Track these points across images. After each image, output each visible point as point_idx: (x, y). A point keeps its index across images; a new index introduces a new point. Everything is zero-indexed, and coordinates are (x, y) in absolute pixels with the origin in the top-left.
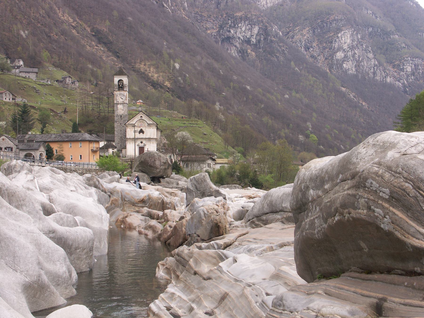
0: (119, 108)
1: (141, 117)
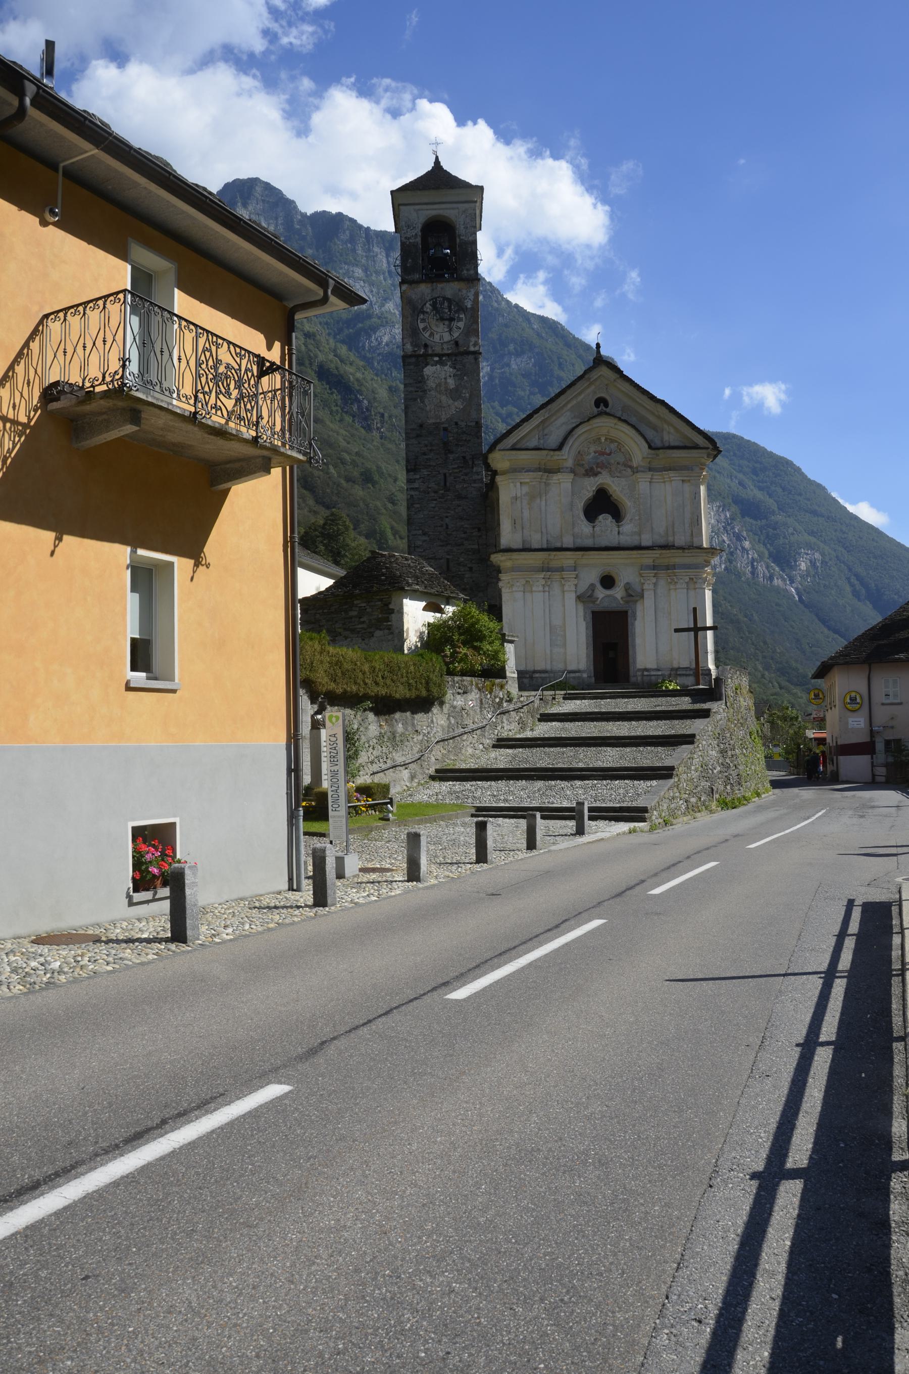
0: (431, 384)
1: (601, 402)
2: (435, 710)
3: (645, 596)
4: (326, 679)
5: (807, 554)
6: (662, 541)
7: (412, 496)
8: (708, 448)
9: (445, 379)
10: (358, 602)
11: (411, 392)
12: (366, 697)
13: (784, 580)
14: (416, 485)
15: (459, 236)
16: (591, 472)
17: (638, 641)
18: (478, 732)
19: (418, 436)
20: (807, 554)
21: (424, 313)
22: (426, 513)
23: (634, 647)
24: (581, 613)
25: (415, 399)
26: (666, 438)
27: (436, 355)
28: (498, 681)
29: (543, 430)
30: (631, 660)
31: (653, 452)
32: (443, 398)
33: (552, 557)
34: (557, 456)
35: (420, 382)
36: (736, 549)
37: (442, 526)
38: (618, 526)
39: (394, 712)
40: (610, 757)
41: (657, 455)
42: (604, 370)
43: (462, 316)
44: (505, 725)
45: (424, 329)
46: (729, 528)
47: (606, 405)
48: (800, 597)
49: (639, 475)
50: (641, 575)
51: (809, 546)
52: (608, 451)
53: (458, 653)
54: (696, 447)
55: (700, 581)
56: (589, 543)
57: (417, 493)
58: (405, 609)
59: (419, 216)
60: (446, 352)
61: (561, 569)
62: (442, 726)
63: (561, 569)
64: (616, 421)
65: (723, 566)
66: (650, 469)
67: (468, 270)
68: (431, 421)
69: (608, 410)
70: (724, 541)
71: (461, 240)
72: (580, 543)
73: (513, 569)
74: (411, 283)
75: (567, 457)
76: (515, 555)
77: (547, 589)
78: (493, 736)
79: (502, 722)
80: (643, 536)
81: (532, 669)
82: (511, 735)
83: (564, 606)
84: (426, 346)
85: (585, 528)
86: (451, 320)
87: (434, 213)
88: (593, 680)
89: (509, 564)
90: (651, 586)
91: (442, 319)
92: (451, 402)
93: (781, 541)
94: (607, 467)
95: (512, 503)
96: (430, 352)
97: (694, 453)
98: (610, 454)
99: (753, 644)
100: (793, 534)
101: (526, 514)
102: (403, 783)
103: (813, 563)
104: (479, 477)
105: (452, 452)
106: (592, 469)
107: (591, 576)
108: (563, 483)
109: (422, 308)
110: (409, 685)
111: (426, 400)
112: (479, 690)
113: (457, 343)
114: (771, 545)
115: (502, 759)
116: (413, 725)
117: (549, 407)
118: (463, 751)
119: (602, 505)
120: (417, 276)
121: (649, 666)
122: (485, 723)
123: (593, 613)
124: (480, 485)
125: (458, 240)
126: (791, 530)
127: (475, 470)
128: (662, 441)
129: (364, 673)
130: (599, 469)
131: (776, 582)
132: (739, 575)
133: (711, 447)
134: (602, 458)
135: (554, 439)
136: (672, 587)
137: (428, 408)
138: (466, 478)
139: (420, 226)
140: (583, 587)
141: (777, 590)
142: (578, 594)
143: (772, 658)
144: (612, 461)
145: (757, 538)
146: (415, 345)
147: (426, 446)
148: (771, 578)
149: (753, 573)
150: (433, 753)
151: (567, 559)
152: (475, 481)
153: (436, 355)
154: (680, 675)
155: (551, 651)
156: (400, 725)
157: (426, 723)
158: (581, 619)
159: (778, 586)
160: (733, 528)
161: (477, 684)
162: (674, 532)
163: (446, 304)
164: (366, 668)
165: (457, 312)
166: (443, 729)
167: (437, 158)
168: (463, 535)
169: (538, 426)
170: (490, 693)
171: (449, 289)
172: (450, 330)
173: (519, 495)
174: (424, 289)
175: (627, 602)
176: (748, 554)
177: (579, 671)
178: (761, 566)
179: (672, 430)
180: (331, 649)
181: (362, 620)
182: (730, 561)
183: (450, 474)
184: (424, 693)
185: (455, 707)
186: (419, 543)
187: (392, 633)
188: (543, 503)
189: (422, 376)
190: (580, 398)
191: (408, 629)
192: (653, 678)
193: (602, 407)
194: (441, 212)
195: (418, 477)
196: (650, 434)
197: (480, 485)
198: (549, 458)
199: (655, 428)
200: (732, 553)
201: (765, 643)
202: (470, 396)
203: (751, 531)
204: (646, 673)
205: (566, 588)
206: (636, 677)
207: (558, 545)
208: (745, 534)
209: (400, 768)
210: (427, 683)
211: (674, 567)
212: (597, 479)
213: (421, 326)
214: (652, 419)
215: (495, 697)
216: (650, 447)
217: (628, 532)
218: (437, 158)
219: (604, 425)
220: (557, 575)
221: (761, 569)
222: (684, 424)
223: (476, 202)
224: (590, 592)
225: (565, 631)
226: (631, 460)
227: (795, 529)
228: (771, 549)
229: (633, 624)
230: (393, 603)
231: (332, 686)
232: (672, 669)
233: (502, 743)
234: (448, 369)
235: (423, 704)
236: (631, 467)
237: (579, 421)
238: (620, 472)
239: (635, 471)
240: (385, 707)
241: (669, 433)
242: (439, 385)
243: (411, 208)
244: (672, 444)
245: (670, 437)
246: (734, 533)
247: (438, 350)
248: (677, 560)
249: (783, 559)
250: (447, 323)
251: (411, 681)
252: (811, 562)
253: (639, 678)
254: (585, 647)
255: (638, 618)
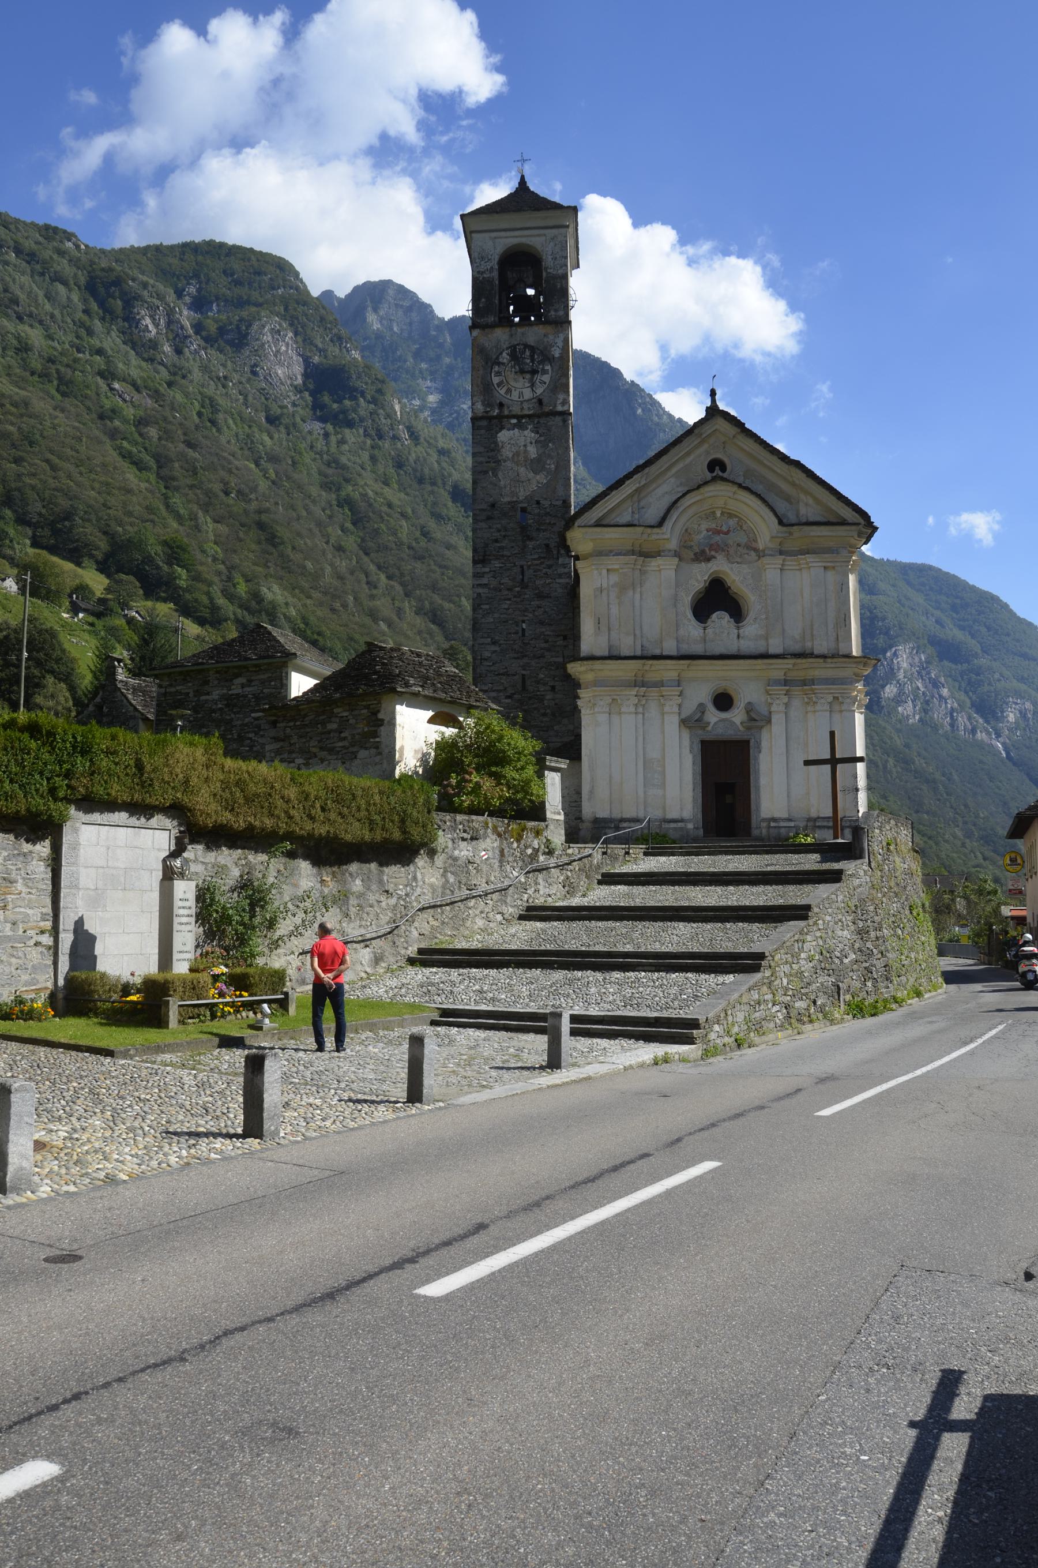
0: (507, 452)
1: (716, 465)
2: (421, 861)
3: (773, 720)
4: (213, 806)
5: (1016, 704)
6: (797, 648)
7: (479, 594)
8: (859, 524)
9: (525, 446)
10: (339, 710)
11: (481, 463)
12: (289, 836)
13: (988, 733)
14: (485, 581)
15: (546, 268)
16: (703, 556)
17: (763, 781)
18: (495, 896)
19: (489, 518)
20: (1016, 704)
21: (499, 364)
22: (496, 615)
23: (758, 788)
24: (686, 742)
25: (486, 472)
26: (803, 510)
27: (514, 417)
28: (531, 824)
29: (639, 501)
30: (753, 807)
31: (785, 529)
32: (522, 470)
33: (647, 668)
34: (656, 534)
35: (492, 450)
36: (933, 697)
37: (516, 633)
38: (738, 628)
39: (348, 861)
40: (678, 937)
41: (791, 534)
42: (720, 423)
43: (548, 367)
44: (541, 887)
45: (499, 385)
46: (924, 673)
47: (723, 468)
48: (1008, 754)
49: (766, 560)
50: (767, 692)
51: (1018, 694)
52: (725, 529)
53: (467, 781)
54: (843, 523)
55: (848, 700)
56: (698, 649)
57: (486, 590)
58: (399, 719)
59: (497, 246)
60: (526, 412)
61: (660, 684)
62: (432, 886)
63: (660, 684)
64: (735, 488)
65: (917, 717)
66: (781, 553)
67: (556, 311)
68: (506, 499)
69: (725, 475)
70: (918, 688)
71: (548, 273)
72: (686, 649)
73: (597, 683)
74: (483, 327)
75: (670, 536)
76: (598, 665)
77: (640, 710)
78: (520, 903)
79: (536, 884)
80: (771, 641)
81: (619, 816)
82: (550, 902)
83: (663, 732)
84: (501, 405)
85: (692, 629)
86: (534, 372)
87: (515, 241)
88: (701, 832)
89: (589, 677)
90: (782, 708)
91: (522, 372)
92: (531, 475)
93: (986, 688)
94: (723, 550)
95: (596, 597)
96: (506, 413)
97: (840, 531)
98: (727, 533)
99: (952, 807)
100: (999, 680)
101: (614, 610)
102: (359, 968)
103: (1023, 714)
104: (566, 570)
105: (531, 539)
106: (703, 552)
107: (701, 694)
108: (664, 570)
109: (497, 358)
110: (371, 822)
111: (500, 475)
112: (499, 835)
113: (540, 402)
114: (974, 692)
115: (521, 936)
116: (381, 882)
117: (647, 470)
118: (468, 923)
119: (716, 599)
120: (491, 319)
121: (777, 815)
122: (506, 883)
123: (703, 742)
124: (567, 580)
125: (544, 274)
126: (997, 676)
127: (560, 561)
128: (797, 516)
129: (288, 802)
130: (713, 553)
131: (980, 736)
132: (935, 728)
133: (862, 522)
134: (717, 538)
135: (653, 514)
136: (809, 708)
137: (502, 483)
138: (549, 571)
139: (497, 258)
140: (690, 708)
141: (981, 746)
142: (683, 716)
143: (975, 825)
144: (731, 542)
145: (957, 684)
146: (488, 404)
147: (499, 531)
148: (973, 731)
149: (952, 725)
150: (416, 924)
151: (668, 670)
152: (560, 576)
153: (514, 417)
154: (819, 827)
155: (645, 792)
156: (358, 882)
157: (404, 881)
158: (686, 751)
159: (982, 740)
160: (929, 673)
161: (495, 828)
162: (812, 635)
163: (528, 353)
164: (292, 793)
165: (541, 362)
166: (434, 891)
167: (523, 177)
168: (544, 645)
169: (631, 495)
170: (518, 841)
171: (533, 335)
172: (532, 386)
173: (605, 585)
174: (500, 335)
175: (749, 728)
176: (946, 703)
177: (682, 820)
178: (962, 717)
179: (811, 501)
180: (229, 763)
181: (343, 735)
182: (926, 711)
183: (529, 567)
184: (397, 835)
185: (456, 859)
186: (487, 654)
187: (380, 754)
188: (638, 596)
189: (496, 443)
190: (688, 460)
191: (402, 748)
192: (783, 831)
193: (717, 472)
194: (524, 240)
195: (487, 570)
196: (781, 506)
197: (567, 580)
198: (645, 537)
199: (788, 499)
200: (927, 702)
201: (966, 806)
202: (557, 467)
203: (950, 676)
204: (772, 824)
205: (667, 709)
206: (759, 829)
207: (657, 652)
208: (942, 680)
209: (355, 945)
210: (403, 821)
211: (812, 682)
212: (710, 565)
213: (496, 380)
214: (784, 486)
215: (526, 847)
216: (781, 523)
217: (751, 634)
218: (523, 177)
219: (720, 495)
220: (654, 692)
221: (962, 720)
222: (827, 493)
223: (568, 227)
224: (699, 715)
225: (664, 767)
226: (755, 541)
227: (1001, 675)
228: (974, 698)
229: (756, 759)
230: (382, 712)
231: (226, 817)
232: (809, 820)
233: (532, 913)
234: (529, 434)
235: (400, 850)
236: (755, 550)
237: (686, 489)
238: (741, 556)
239: (760, 554)
240: (329, 853)
241: (807, 504)
242: (517, 454)
243: (486, 235)
244: (811, 519)
245: (808, 510)
246: (930, 679)
247: (516, 410)
248: (818, 673)
249: (988, 709)
250: (528, 376)
251: (376, 817)
252: (1021, 712)
253: (764, 831)
254: (691, 787)
255: (763, 750)
